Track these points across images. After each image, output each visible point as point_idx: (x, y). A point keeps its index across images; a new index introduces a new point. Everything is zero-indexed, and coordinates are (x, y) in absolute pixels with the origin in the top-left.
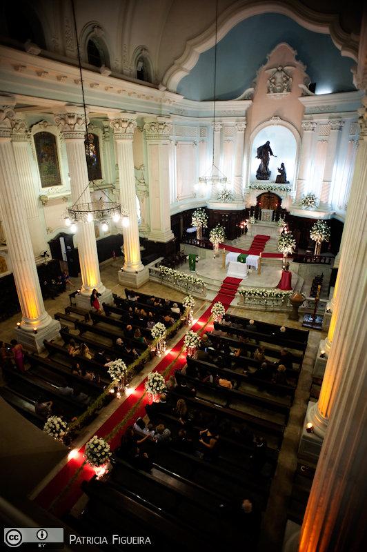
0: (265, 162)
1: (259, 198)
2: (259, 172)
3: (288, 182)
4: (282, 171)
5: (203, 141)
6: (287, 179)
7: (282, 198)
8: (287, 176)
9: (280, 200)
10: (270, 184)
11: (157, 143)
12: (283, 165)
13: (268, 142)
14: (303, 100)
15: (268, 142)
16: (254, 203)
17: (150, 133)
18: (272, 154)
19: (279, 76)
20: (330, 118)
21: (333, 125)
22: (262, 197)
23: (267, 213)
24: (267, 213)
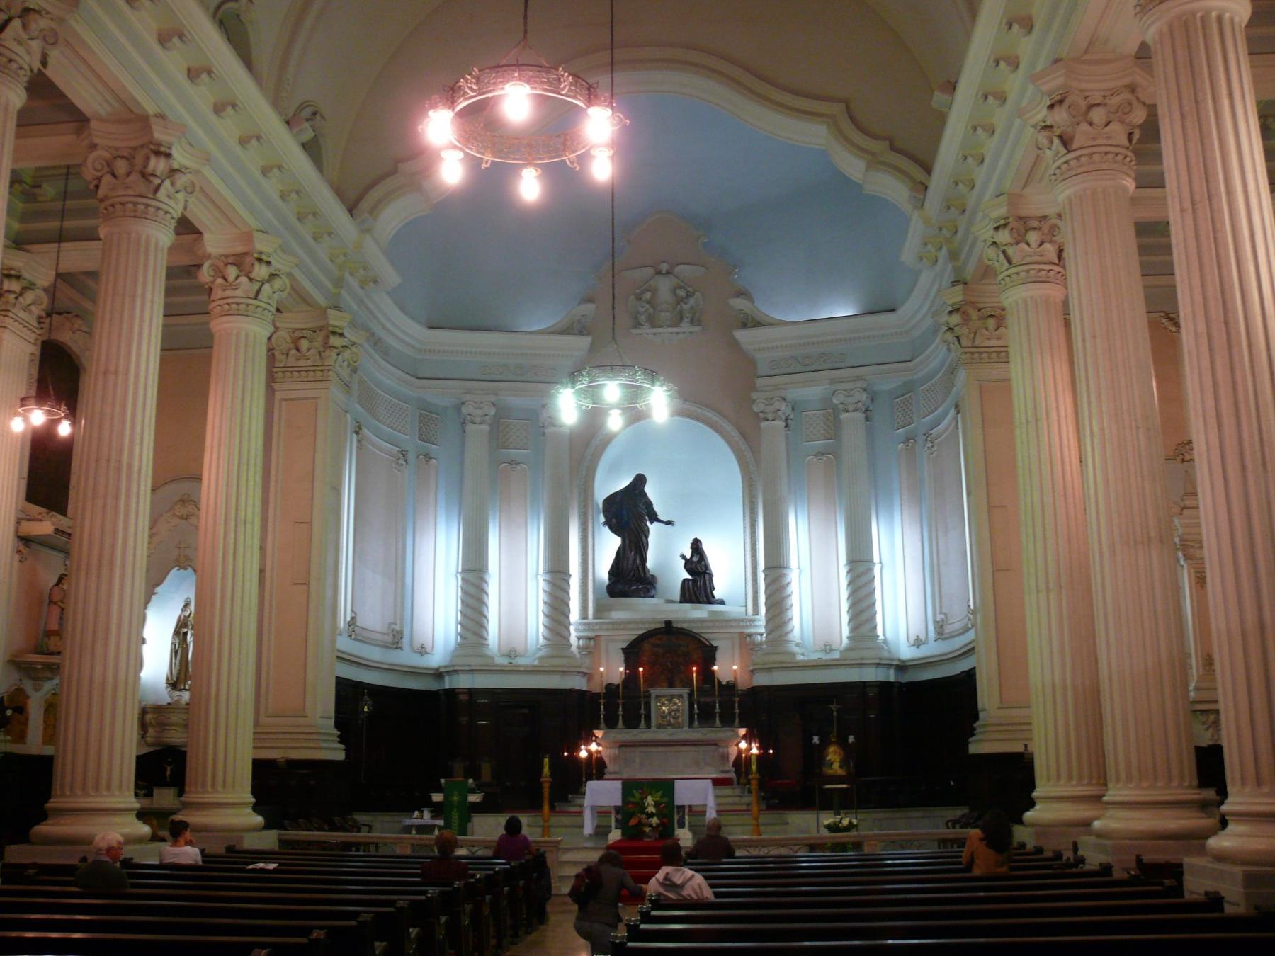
0: (634, 545)
1: (632, 653)
2: (616, 571)
3: (722, 602)
4: (698, 565)
5: (428, 457)
6: (718, 594)
7: (714, 644)
8: (714, 579)
9: (708, 654)
10: (662, 606)
11: (311, 394)
12: (696, 546)
13: (640, 481)
14: (742, 336)
15: (640, 481)
16: (613, 670)
17: (291, 361)
18: (654, 518)
19: (664, 286)
20: (833, 381)
21: (848, 400)
22: (647, 646)
23: (669, 703)
24: (669, 703)
